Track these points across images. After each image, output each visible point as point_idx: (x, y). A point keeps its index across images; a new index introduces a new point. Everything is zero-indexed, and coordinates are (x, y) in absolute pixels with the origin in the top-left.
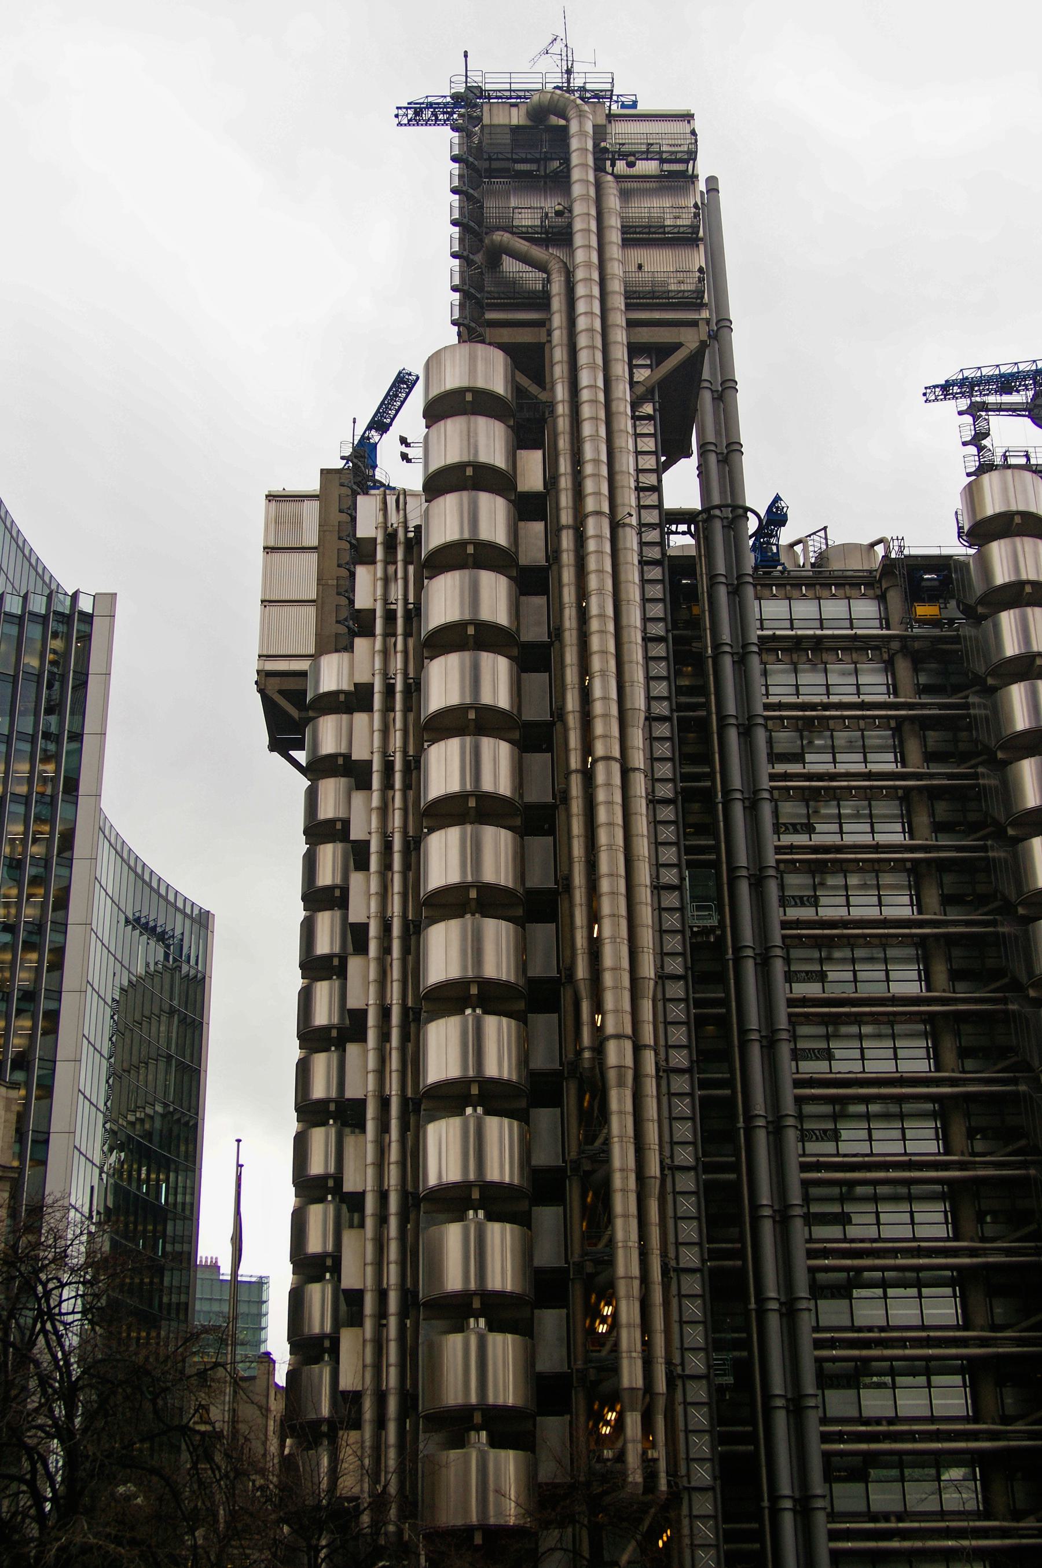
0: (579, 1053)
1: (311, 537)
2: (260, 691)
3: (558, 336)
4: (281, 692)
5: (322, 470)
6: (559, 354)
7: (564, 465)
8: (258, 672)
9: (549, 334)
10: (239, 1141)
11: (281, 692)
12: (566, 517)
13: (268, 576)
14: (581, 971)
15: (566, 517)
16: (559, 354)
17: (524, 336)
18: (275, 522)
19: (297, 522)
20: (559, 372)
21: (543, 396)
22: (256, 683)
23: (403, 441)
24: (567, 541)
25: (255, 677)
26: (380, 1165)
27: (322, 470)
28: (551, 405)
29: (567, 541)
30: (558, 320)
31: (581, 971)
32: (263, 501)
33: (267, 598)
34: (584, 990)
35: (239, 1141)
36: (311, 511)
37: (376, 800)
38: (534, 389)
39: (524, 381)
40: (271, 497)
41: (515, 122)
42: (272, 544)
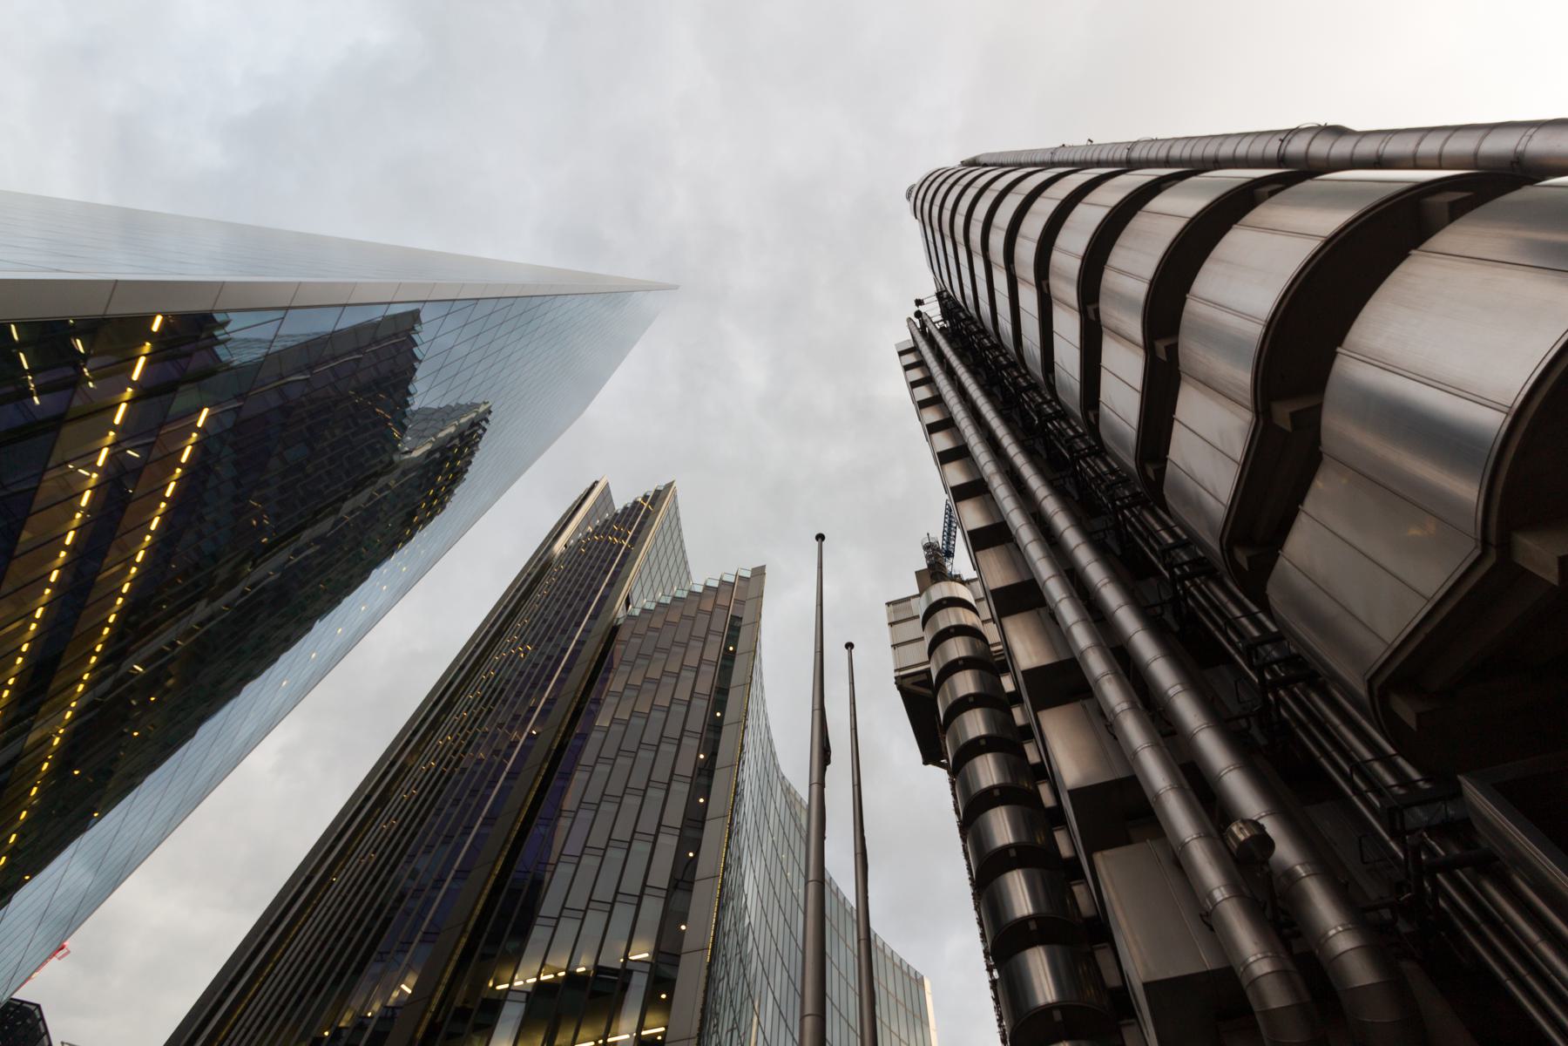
2: (900, 688)
4: (914, 684)
5: (916, 572)
8: (896, 678)
10: (820, 537)
11: (914, 684)
13: (893, 635)
18: (895, 612)
19: (910, 608)
22: (896, 683)
23: (919, 302)
25: (894, 680)
27: (916, 572)
32: (885, 607)
33: (895, 643)
35: (820, 537)
40: (888, 604)
42: (893, 620)
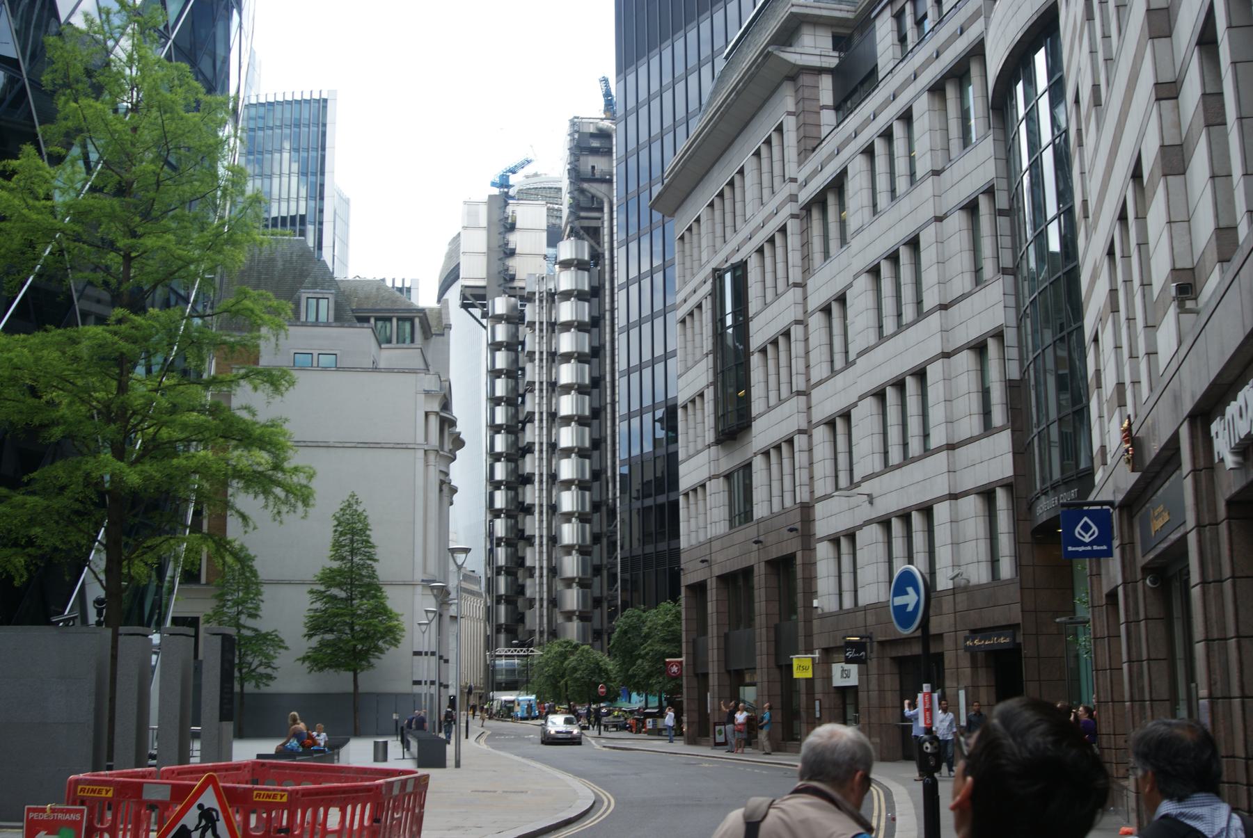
0: (608, 499)
1: (483, 222)
3: (606, 231)
6: (606, 239)
7: (607, 286)
9: (603, 223)
12: (608, 307)
14: (609, 474)
15: (608, 307)
16: (606, 239)
17: (593, 224)
20: (606, 246)
21: (600, 250)
24: (608, 316)
26: (540, 528)
28: (604, 257)
29: (608, 316)
30: (606, 224)
31: (609, 474)
34: (610, 480)
36: (483, 211)
37: (537, 400)
38: (596, 246)
39: (594, 244)
40: (465, 203)
41: (591, 131)
